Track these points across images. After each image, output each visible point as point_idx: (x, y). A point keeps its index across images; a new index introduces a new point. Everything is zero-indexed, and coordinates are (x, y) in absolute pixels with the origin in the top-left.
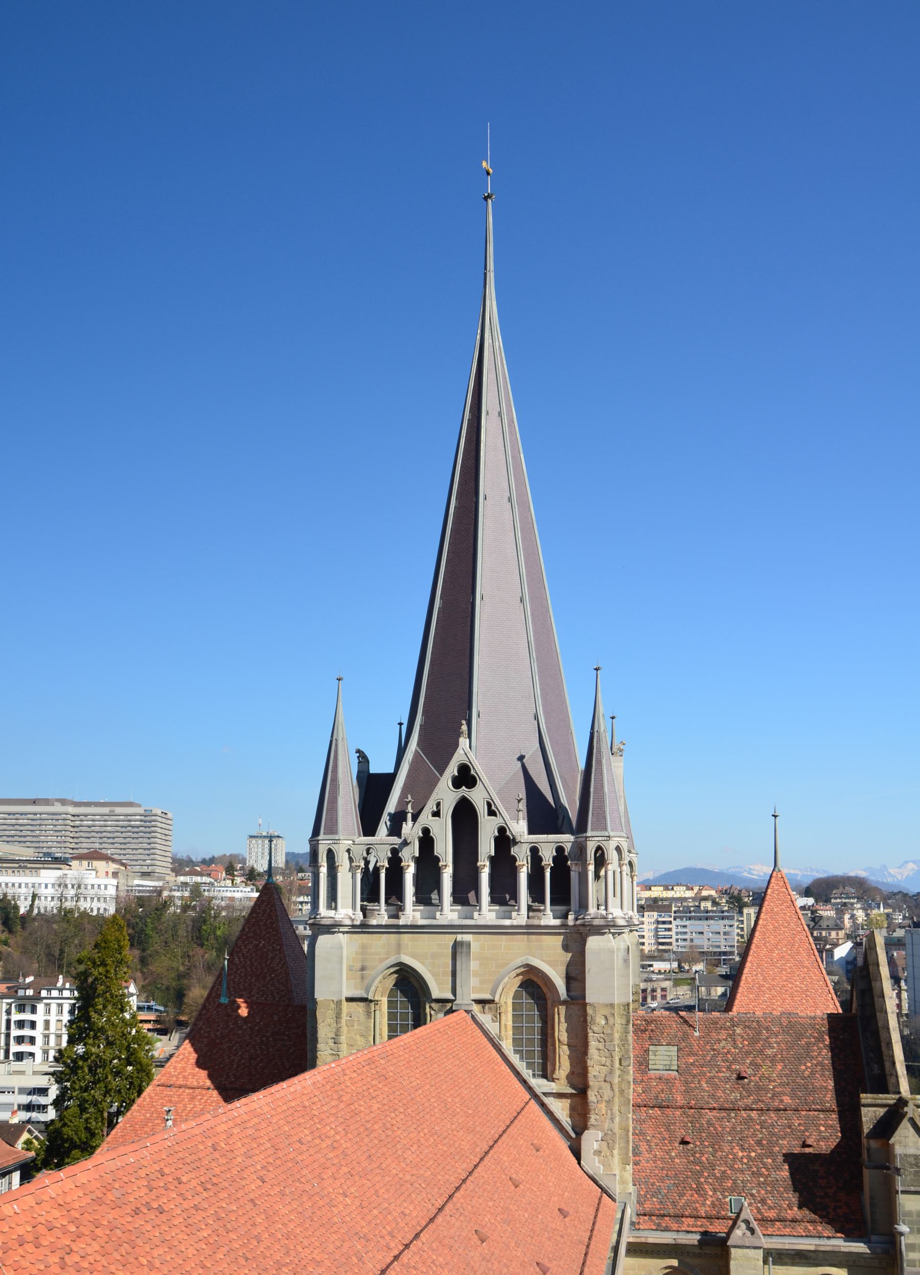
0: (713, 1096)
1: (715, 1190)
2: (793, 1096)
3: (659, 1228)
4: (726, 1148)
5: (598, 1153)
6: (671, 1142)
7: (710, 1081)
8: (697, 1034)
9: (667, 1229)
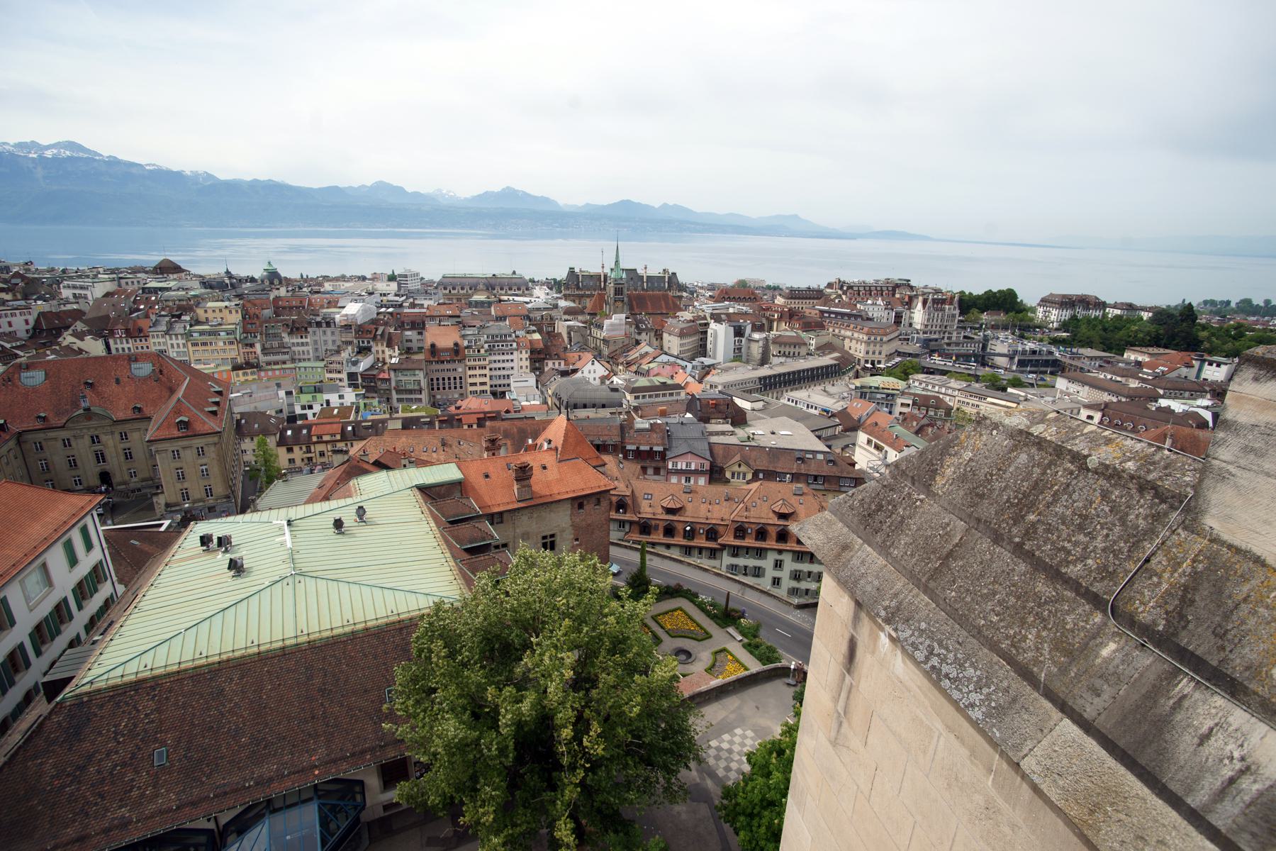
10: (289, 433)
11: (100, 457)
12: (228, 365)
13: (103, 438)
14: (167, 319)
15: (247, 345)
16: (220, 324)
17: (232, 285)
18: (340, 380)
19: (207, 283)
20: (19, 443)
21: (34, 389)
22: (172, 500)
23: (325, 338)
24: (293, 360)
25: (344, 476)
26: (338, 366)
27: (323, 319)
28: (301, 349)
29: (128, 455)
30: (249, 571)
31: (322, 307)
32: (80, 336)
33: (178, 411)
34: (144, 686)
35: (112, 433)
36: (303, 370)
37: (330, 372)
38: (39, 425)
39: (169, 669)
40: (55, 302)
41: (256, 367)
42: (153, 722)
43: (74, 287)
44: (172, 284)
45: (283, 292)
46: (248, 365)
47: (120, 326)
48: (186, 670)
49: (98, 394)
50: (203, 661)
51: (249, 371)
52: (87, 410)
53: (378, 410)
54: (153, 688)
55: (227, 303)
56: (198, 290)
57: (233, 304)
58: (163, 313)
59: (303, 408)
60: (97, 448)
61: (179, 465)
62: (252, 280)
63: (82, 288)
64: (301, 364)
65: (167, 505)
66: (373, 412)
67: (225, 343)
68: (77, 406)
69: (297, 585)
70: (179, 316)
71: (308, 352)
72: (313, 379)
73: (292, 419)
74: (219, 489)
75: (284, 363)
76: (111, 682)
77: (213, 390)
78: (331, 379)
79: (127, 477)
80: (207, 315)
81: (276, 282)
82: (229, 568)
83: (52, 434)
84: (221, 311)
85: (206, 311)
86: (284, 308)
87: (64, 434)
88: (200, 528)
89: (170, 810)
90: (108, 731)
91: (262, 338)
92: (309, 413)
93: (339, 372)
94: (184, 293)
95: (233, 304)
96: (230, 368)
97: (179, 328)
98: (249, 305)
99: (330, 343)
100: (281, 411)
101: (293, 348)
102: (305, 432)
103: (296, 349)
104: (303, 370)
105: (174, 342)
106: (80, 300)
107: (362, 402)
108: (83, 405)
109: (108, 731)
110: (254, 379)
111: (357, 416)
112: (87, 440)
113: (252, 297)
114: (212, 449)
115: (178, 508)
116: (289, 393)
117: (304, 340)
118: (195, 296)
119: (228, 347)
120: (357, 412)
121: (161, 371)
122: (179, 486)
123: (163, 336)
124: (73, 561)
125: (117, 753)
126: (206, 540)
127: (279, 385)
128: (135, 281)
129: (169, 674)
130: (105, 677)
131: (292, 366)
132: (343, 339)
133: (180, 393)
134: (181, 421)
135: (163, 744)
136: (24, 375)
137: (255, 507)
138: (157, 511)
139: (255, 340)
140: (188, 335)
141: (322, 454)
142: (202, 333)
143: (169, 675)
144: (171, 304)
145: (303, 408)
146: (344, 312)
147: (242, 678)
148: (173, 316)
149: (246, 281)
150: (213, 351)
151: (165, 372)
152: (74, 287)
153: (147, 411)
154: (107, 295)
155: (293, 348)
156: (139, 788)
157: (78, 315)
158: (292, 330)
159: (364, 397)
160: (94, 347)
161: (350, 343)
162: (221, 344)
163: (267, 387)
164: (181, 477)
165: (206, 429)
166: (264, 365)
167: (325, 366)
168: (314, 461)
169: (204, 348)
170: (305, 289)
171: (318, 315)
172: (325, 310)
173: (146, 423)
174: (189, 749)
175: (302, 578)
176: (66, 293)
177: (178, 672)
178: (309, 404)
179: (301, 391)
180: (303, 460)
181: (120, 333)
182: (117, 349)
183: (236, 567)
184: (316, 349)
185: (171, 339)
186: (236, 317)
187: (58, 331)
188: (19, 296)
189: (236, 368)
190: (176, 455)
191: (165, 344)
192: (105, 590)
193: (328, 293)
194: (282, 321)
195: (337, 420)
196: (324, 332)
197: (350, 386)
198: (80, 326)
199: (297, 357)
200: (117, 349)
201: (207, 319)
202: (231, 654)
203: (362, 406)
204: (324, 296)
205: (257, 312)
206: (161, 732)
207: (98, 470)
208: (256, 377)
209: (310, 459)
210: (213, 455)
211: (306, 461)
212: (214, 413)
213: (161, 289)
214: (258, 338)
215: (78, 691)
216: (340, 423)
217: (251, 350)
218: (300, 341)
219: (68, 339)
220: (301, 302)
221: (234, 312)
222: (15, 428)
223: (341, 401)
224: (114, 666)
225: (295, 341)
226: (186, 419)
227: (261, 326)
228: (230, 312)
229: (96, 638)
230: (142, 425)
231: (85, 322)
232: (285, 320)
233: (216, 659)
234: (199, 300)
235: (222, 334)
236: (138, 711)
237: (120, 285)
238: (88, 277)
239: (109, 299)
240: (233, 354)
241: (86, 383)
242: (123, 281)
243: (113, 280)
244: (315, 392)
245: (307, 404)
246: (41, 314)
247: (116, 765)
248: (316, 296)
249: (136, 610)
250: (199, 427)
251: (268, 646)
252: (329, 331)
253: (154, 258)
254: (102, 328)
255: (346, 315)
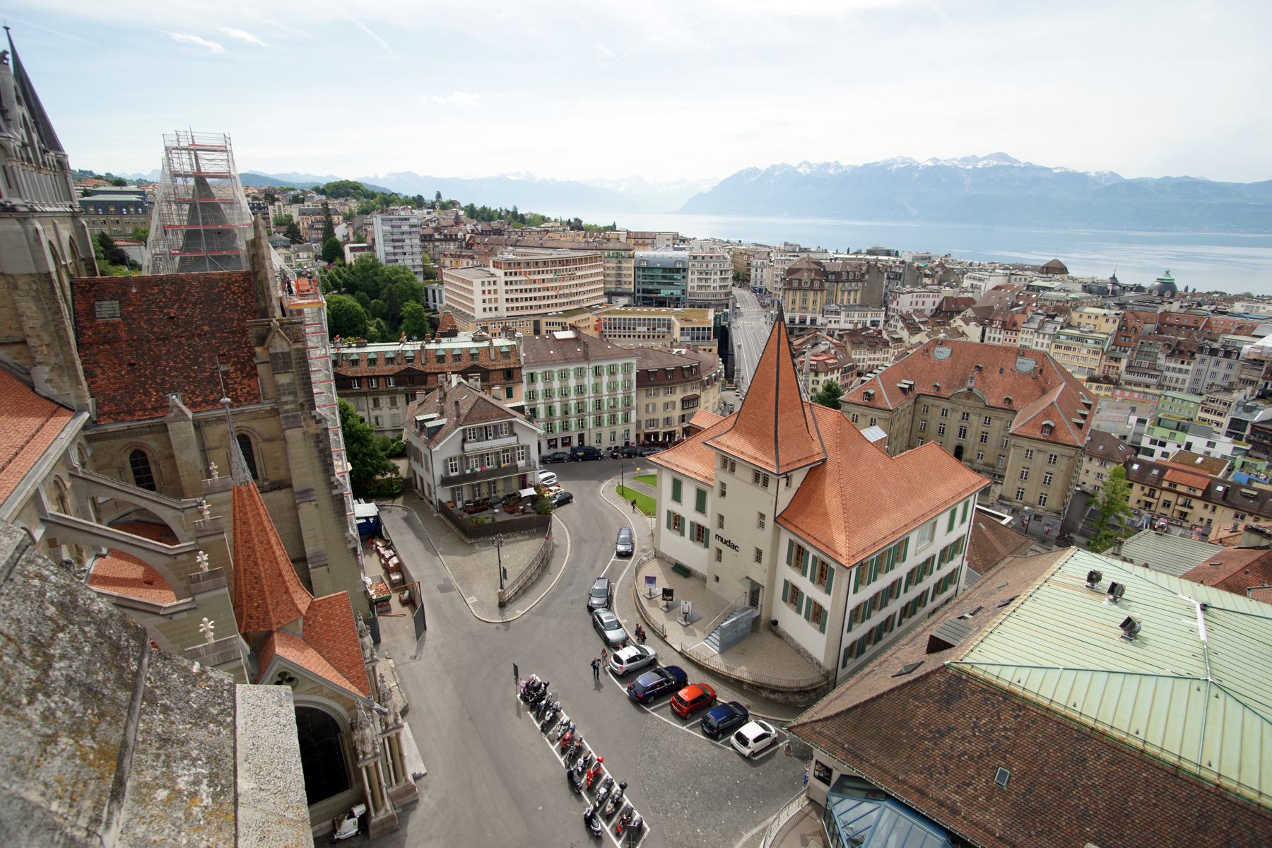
0: (152, 332)
1: (157, 392)
2: (210, 325)
3: (116, 421)
4: (164, 363)
5: (48, 381)
6: (120, 365)
7: (147, 322)
8: (134, 291)
9: (123, 421)
10: (1136, 467)
11: (963, 433)
12: (1083, 373)
13: (972, 417)
14: (1042, 317)
15: (1112, 358)
16: (1092, 332)
17: (1113, 292)
18: (1218, 424)
19: (1086, 288)
20: (915, 402)
21: (940, 363)
22: (1005, 494)
23: (1215, 370)
24: (1160, 386)
25: (1256, 565)
26: (1221, 406)
27: (1222, 346)
28: (1175, 375)
29: (984, 439)
30: (1143, 643)
31: (1227, 332)
32: (967, 321)
33: (1047, 414)
34: (1013, 700)
35: (980, 415)
36: (1169, 400)
37: (1207, 411)
38: (932, 392)
39: (1040, 699)
40: (957, 290)
41: (1114, 384)
42: (1007, 738)
43: (975, 279)
44: (1056, 285)
45: (1175, 307)
46: (1107, 380)
47: (1000, 318)
48: (1055, 712)
49: (983, 379)
50: (1075, 715)
51: (1104, 386)
52: (970, 389)
53: (1263, 477)
54: (1020, 708)
55: (1106, 311)
56: (1079, 294)
57: (1114, 312)
58: (1040, 311)
59: (1153, 442)
60: (964, 424)
61: (1027, 465)
62: (1139, 289)
63: (980, 280)
64: (1169, 393)
65: (1001, 497)
66: (1253, 477)
67: (1089, 352)
68: (963, 384)
69: (1213, 698)
70: (1053, 317)
71: (1184, 381)
72: (1180, 414)
73: (1138, 449)
74: (1053, 502)
75: (1148, 386)
76: (988, 676)
77: (1082, 401)
78: (1204, 420)
79: (975, 457)
80: (1080, 320)
81: (1168, 294)
82: (1123, 626)
83: (938, 402)
84: (1097, 317)
85: (1081, 316)
86: (1171, 325)
87: (946, 405)
88: (1079, 561)
89: (992, 834)
90: (971, 718)
91: (1132, 354)
92: (1158, 450)
93: (1220, 414)
94: (1064, 294)
95: (1114, 312)
96: (1085, 377)
97: (1049, 328)
98: (1131, 316)
99: (1220, 376)
100: (1125, 437)
101: (1166, 373)
102: (1155, 472)
103: (1168, 374)
104: (1169, 400)
105: (1040, 340)
106: (976, 291)
107: (1240, 460)
108: (970, 385)
109: (971, 718)
110: (1106, 396)
111: (1229, 474)
112: (960, 415)
113: (1136, 308)
114: (1065, 461)
115: (1008, 503)
116: (1141, 421)
117: (1184, 367)
118: (1074, 299)
119: (1091, 356)
120: (1230, 470)
121: (1041, 370)
122: (1019, 484)
123: (1032, 333)
124: (950, 528)
125: (970, 742)
126: (1094, 577)
127: (1133, 410)
128: (1023, 278)
129: (1038, 705)
130: (984, 667)
131: (1158, 392)
132: (1243, 376)
133: (1054, 396)
134: (1048, 425)
135: (1009, 766)
136: (937, 349)
137: (1119, 549)
138: (991, 498)
139: (1124, 354)
140: (1056, 337)
141: (1167, 504)
142: (1069, 337)
143: (1038, 705)
144: (1048, 303)
145: (1153, 442)
146: (1260, 342)
147: (1112, 763)
148: (1048, 316)
149: (1131, 289)
150: (1073, 357)
151: (1044, 372)
152: (975, 279)
153: (1015, 405)
154: (997, 288)
155: (1166, 373)
156: (975, 789)
157: (969, 302)
158: (1173, 352)
159: (1247, 454)
160: (973, 332)
161: (1252, 383)
162: (1085, 351)
163: (1118, 408)
164: (1024, 476)
165: (1068, 440)
166: (1123, 383)
167: (1202, 403)
168: (1153, 508)
169: (1066, 352)
170: (1205, 307)
171: (1216, 341)
172: (1229, 337)
173: (1010, 415)
174: (1029, 791)
175: (1222, 695)
176: (966, 283)
177: (1048, 709)
178: (1163, 440)
179: (1159, 422)
180: (1139, 501)
181: (997, 323)
182: (989, 338)
183: (1129, 627)
184: (1197, 380)
185: (1038, 337)
186: (1112, 328)
187: (951, 314)
188: (936, 282)
189: (1092, 379)
190: (1029, 454)
191: (1031, 340)
192: (957, 561)
193: (1239, 315)
194: (1165, 339)
195: (1202, 472)
196: (1217, 363)
197: (1228, 434)
198: (969, 312)
199: (1167, 383)
200: (989, 338)
201: (1079, 324)
202: (1108, 729)
203: (1238, 464)
204: (1232, 318)
205: (1137, 325)
206: (1011, 754)
207: (956, 443)
208: (1109, 393)
209: (1148, 504)
210: (1063, 468)
211: (1142, 504)
212: (1080, 426)
213: (1044, 288)
214: (1128, 353)
215: (960, 666)
216: (1207, 477)
217: (1115, 364)
218: (1179, 366)
219: (957, 322)
220: (1196, 322)
221: (1111, 321)
222: (917, 390)
223: (1209, 449)
224: (992, 662)
225: (1172, 365)
226: (1053, 425)
227: (1136, 341)
228: (1107, 321)
229: (967, 615)
230: (1007, 416)
231: (973, 309)
232: (1169, 339)
233: (1091, 723)
234: (1077, 304)
235: (1089, 341)
236: (999, 719)
237: (1009, 281)
238: (986, 270)
239: (997, 292)
240: (1093, 365)
241: (978, 367)
242: (1013, 277)
243: (1006, 275)
244: (1177, 429)
245: (1159, 439)
246: (946, 298)
247: (965, 753)
248: (1220, 317)
249: (1014, 615)
250: (1061, 436)
251: (1158, 751)
252: (1225, 362)
253: (1043, 259)
254: (985, 318)
255: (1262, 348)
